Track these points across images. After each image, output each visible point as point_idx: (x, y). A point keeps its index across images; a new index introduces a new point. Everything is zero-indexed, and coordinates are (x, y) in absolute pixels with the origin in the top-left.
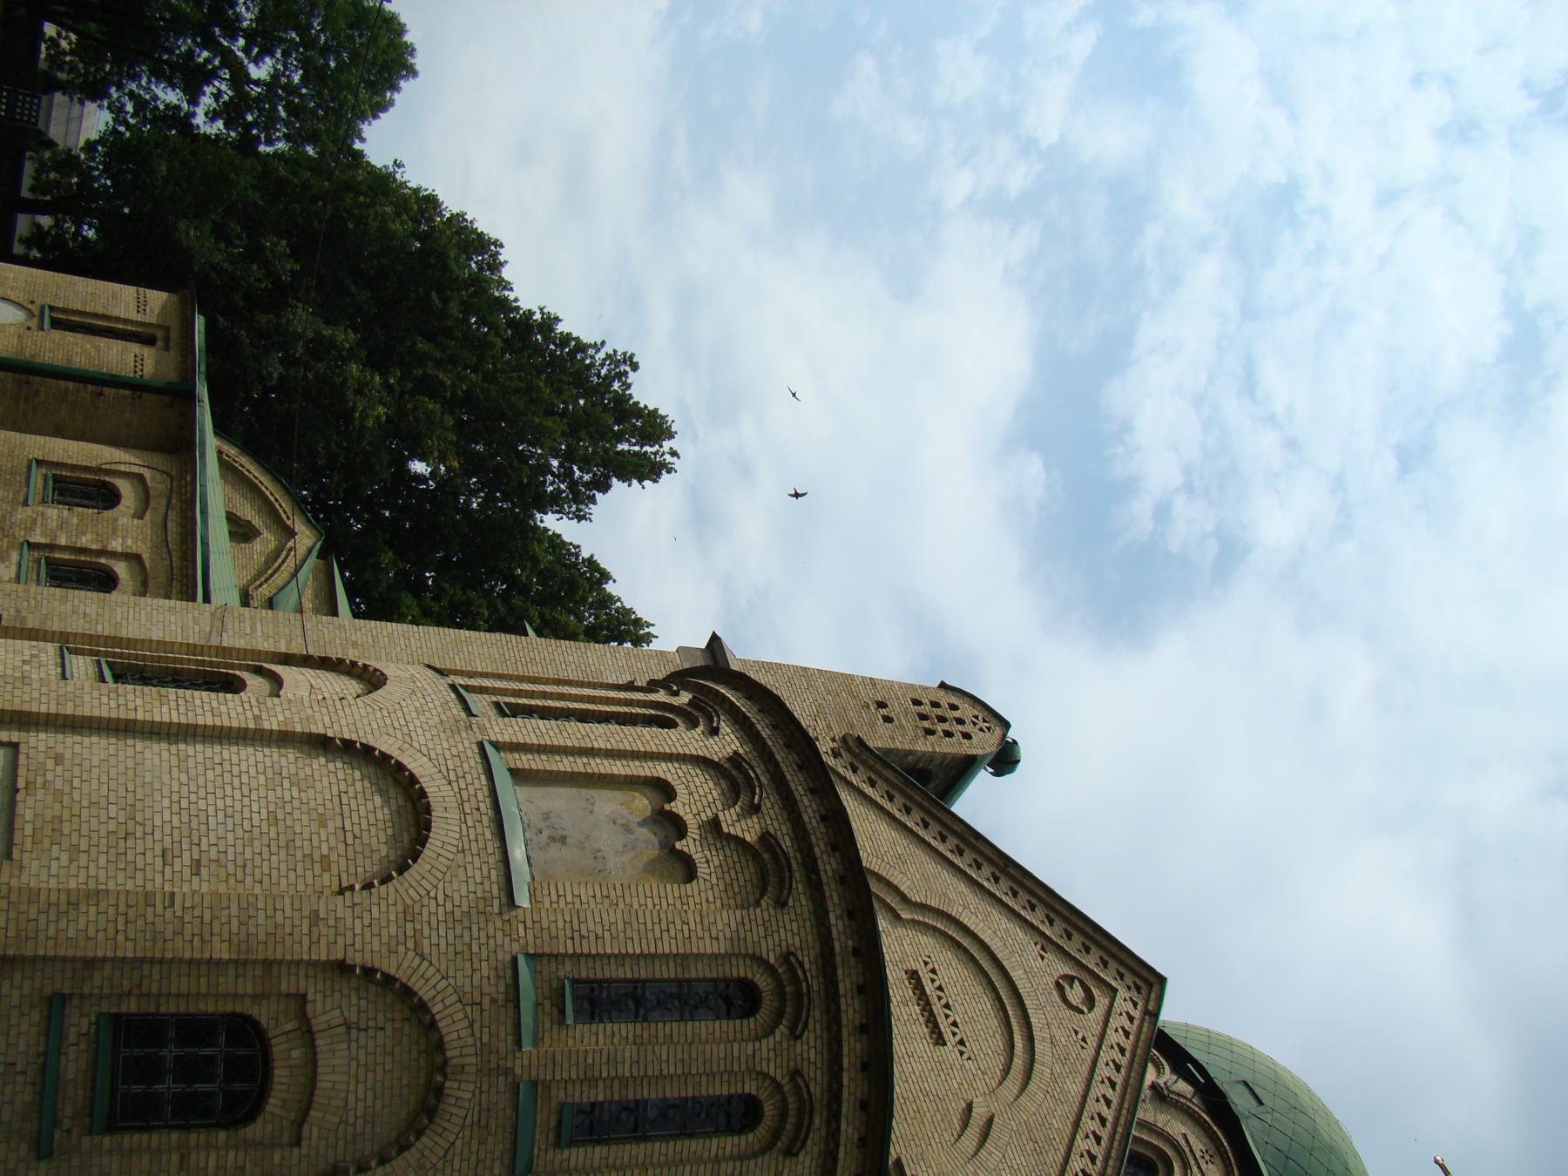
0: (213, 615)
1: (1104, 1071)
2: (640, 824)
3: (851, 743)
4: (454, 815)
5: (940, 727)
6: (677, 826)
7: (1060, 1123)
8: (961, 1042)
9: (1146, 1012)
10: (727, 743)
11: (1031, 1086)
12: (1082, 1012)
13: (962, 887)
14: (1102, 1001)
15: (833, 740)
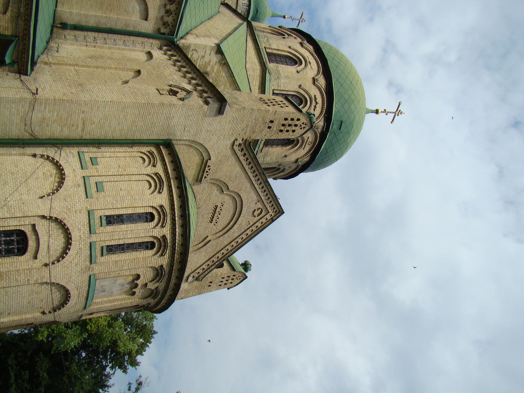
0: (30, 103)
1: (248, 232)
2: (128, 283)
3: (247, 143)
4: (76, 297)
5: (290, 122)
6: (136, 286)
7: (226, 243)
8: (216, 223)
9: (272, 219)
10: (164, 261)
11: (226, 235)
12: (255, 216)
13: (249, 185)
14: (263, 214)
15: (243, 139)
